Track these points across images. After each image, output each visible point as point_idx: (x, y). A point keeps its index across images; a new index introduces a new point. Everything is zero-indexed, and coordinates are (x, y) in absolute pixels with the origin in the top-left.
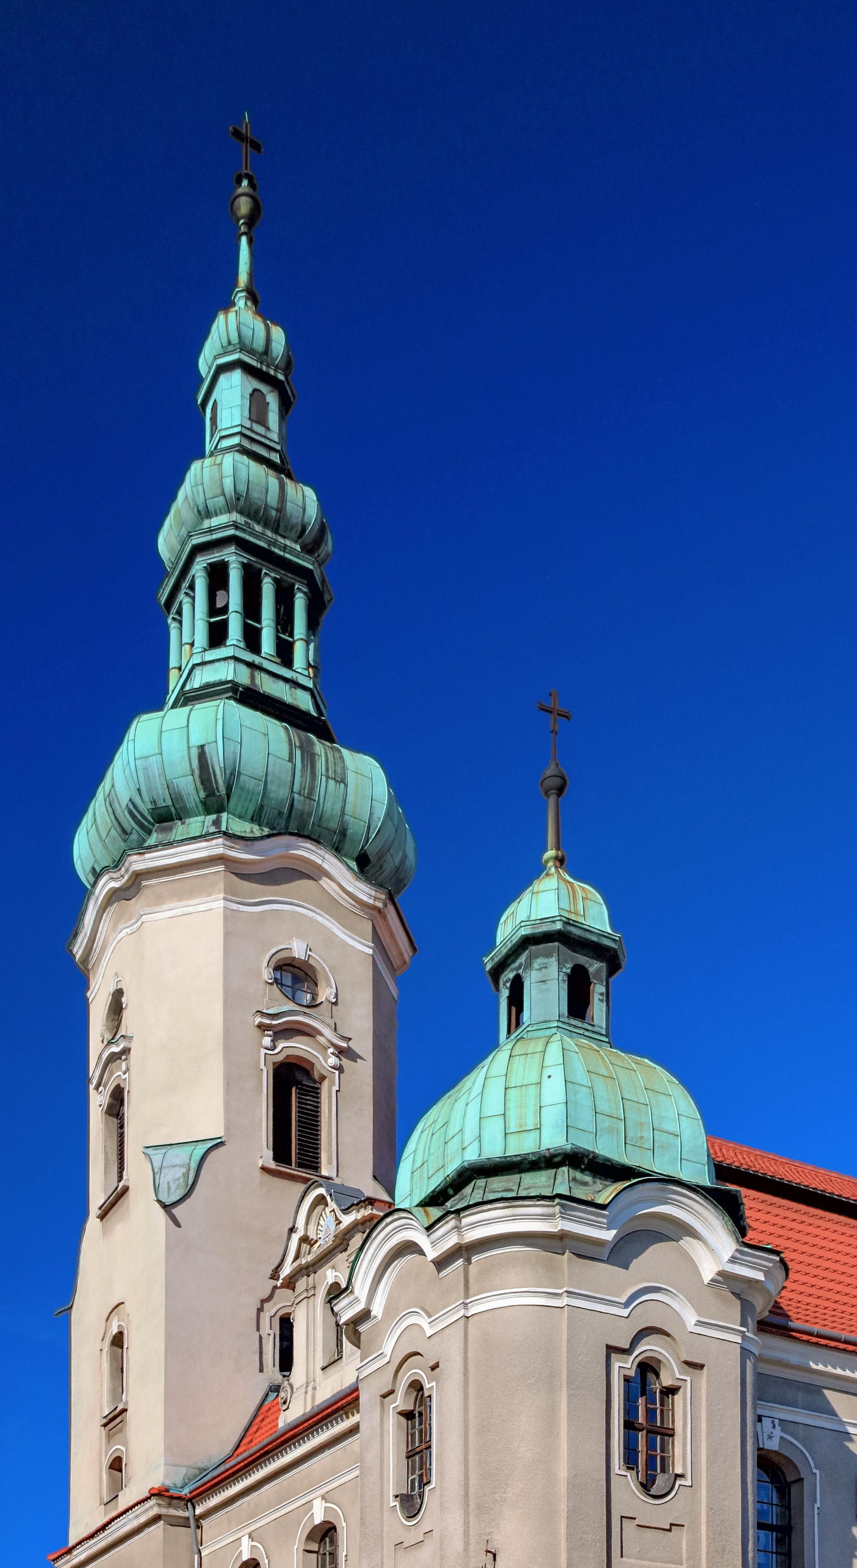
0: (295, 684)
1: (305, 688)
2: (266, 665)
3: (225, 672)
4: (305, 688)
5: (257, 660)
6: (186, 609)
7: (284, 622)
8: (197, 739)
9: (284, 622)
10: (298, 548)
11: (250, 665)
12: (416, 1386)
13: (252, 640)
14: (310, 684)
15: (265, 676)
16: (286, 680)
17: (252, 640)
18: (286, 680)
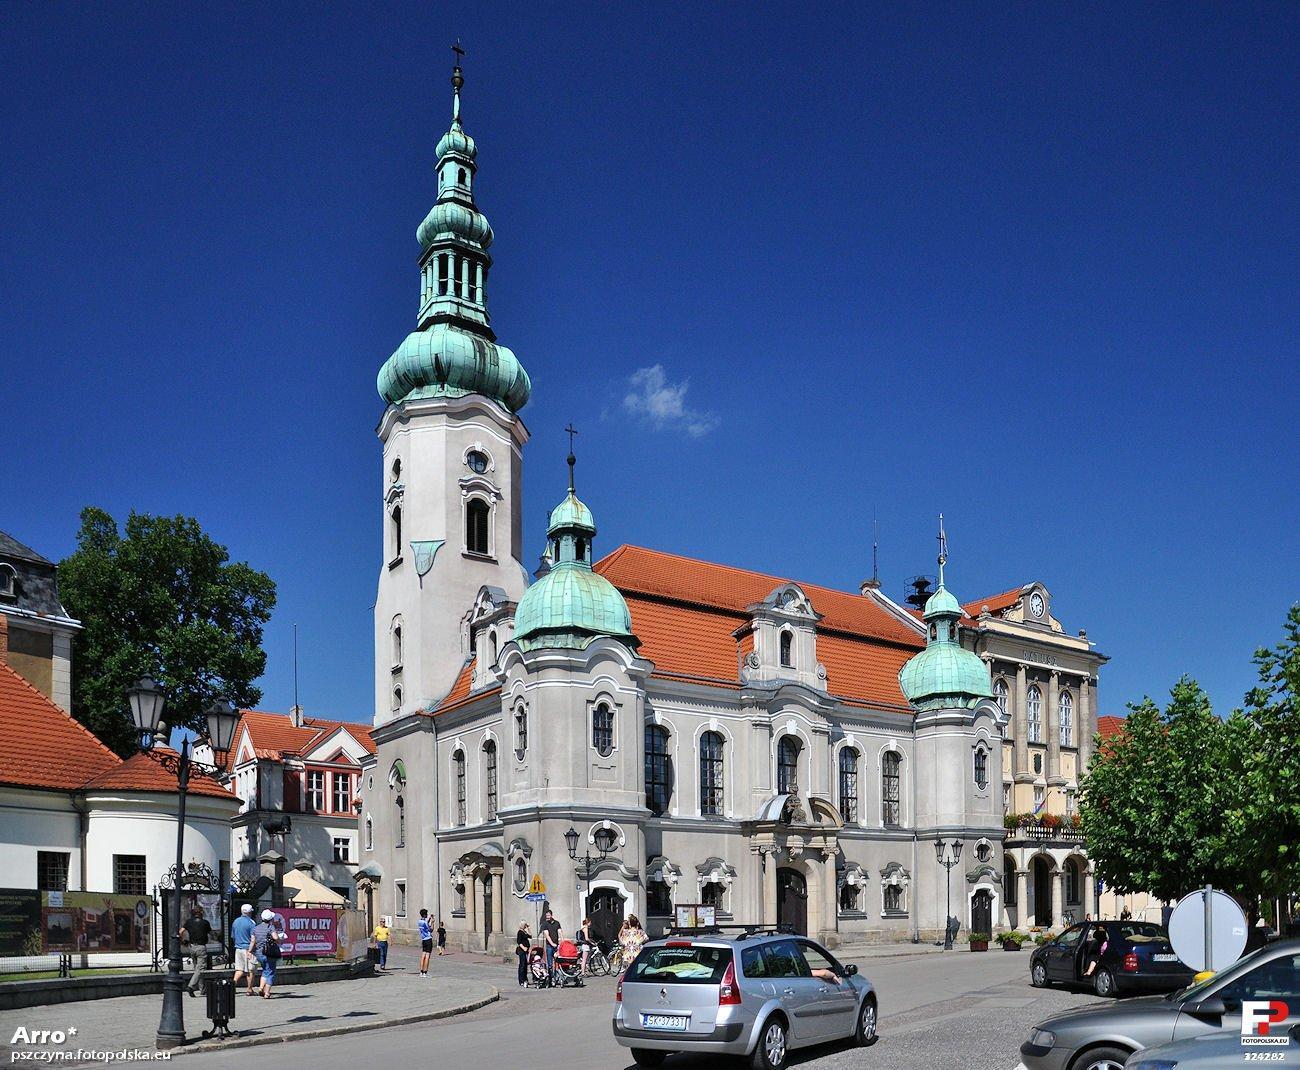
0: (476, 310)
1: (481, 312)
2: (464, 302)
3: (449, 309)
4: (481, 312)
5: (460, 301)
6: (429, 270)
7: (472, 280)
8: (434, 352)
9: (472, 280)
10: (479, 246)
11: (458, 304)
12: (521, 710)
13: (458, 289)
14: (483, 309)
15: (465, 309)
16: (473, 309)
17: (458, 289)
18: (473, 309)
